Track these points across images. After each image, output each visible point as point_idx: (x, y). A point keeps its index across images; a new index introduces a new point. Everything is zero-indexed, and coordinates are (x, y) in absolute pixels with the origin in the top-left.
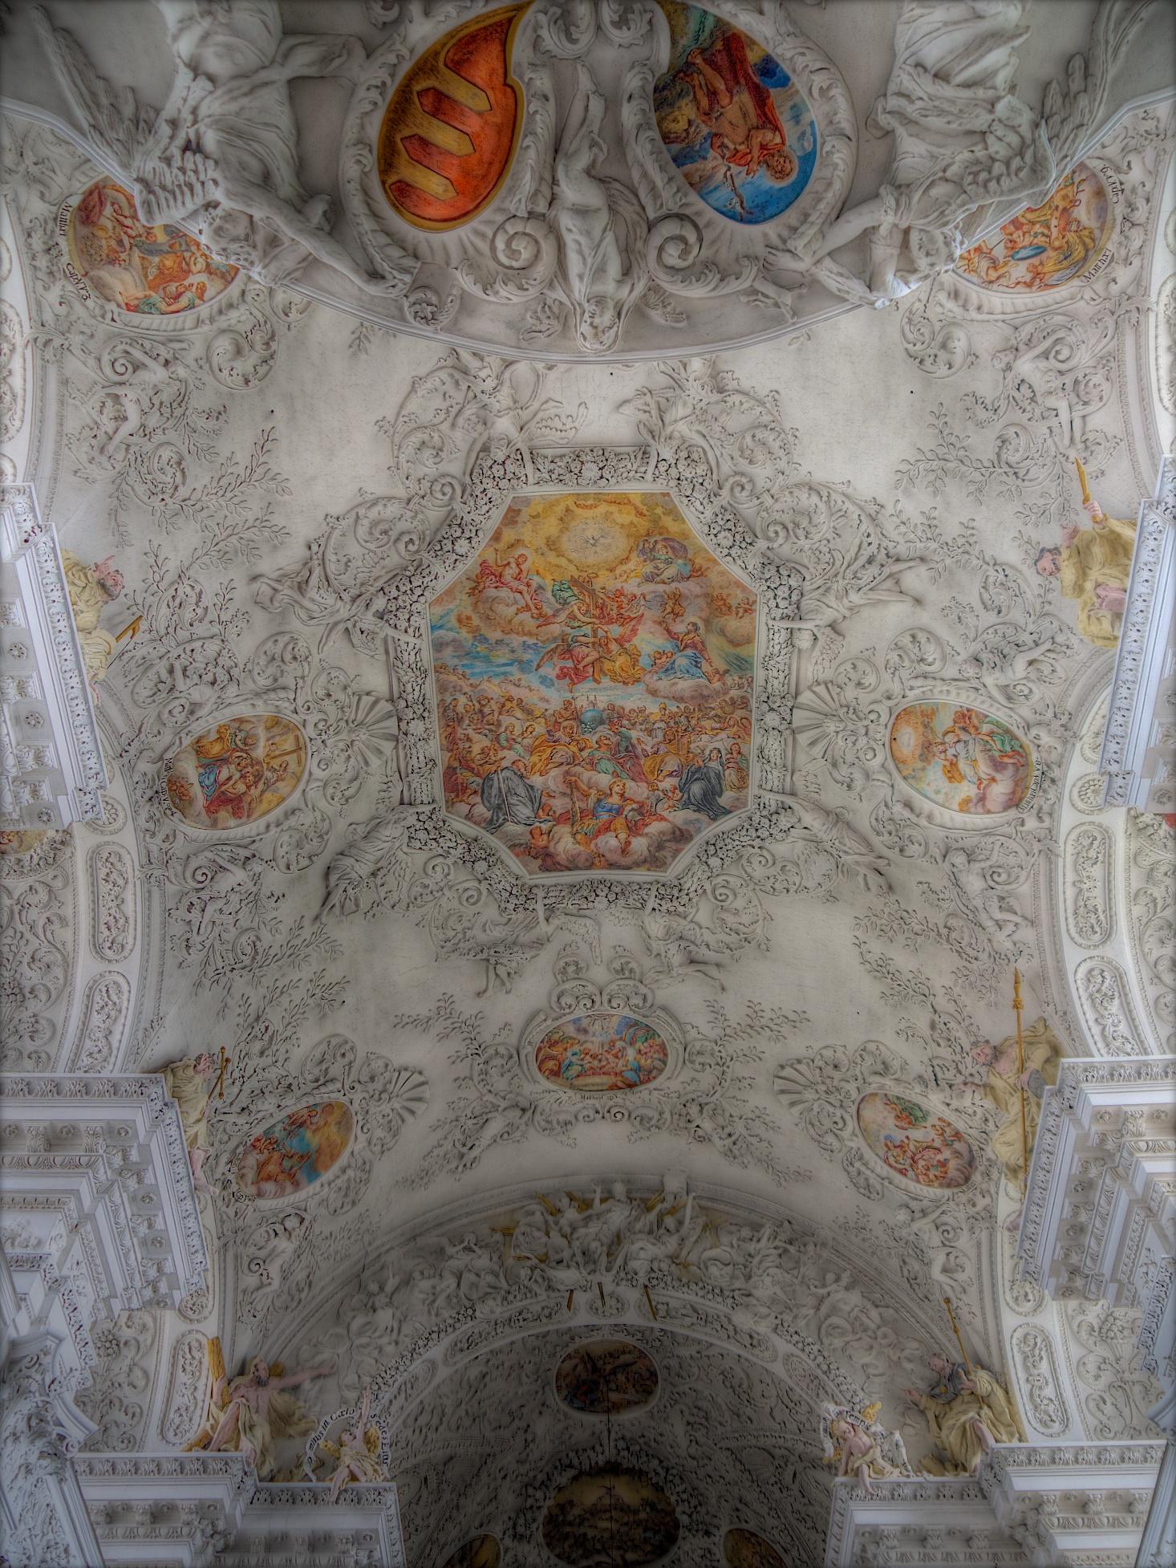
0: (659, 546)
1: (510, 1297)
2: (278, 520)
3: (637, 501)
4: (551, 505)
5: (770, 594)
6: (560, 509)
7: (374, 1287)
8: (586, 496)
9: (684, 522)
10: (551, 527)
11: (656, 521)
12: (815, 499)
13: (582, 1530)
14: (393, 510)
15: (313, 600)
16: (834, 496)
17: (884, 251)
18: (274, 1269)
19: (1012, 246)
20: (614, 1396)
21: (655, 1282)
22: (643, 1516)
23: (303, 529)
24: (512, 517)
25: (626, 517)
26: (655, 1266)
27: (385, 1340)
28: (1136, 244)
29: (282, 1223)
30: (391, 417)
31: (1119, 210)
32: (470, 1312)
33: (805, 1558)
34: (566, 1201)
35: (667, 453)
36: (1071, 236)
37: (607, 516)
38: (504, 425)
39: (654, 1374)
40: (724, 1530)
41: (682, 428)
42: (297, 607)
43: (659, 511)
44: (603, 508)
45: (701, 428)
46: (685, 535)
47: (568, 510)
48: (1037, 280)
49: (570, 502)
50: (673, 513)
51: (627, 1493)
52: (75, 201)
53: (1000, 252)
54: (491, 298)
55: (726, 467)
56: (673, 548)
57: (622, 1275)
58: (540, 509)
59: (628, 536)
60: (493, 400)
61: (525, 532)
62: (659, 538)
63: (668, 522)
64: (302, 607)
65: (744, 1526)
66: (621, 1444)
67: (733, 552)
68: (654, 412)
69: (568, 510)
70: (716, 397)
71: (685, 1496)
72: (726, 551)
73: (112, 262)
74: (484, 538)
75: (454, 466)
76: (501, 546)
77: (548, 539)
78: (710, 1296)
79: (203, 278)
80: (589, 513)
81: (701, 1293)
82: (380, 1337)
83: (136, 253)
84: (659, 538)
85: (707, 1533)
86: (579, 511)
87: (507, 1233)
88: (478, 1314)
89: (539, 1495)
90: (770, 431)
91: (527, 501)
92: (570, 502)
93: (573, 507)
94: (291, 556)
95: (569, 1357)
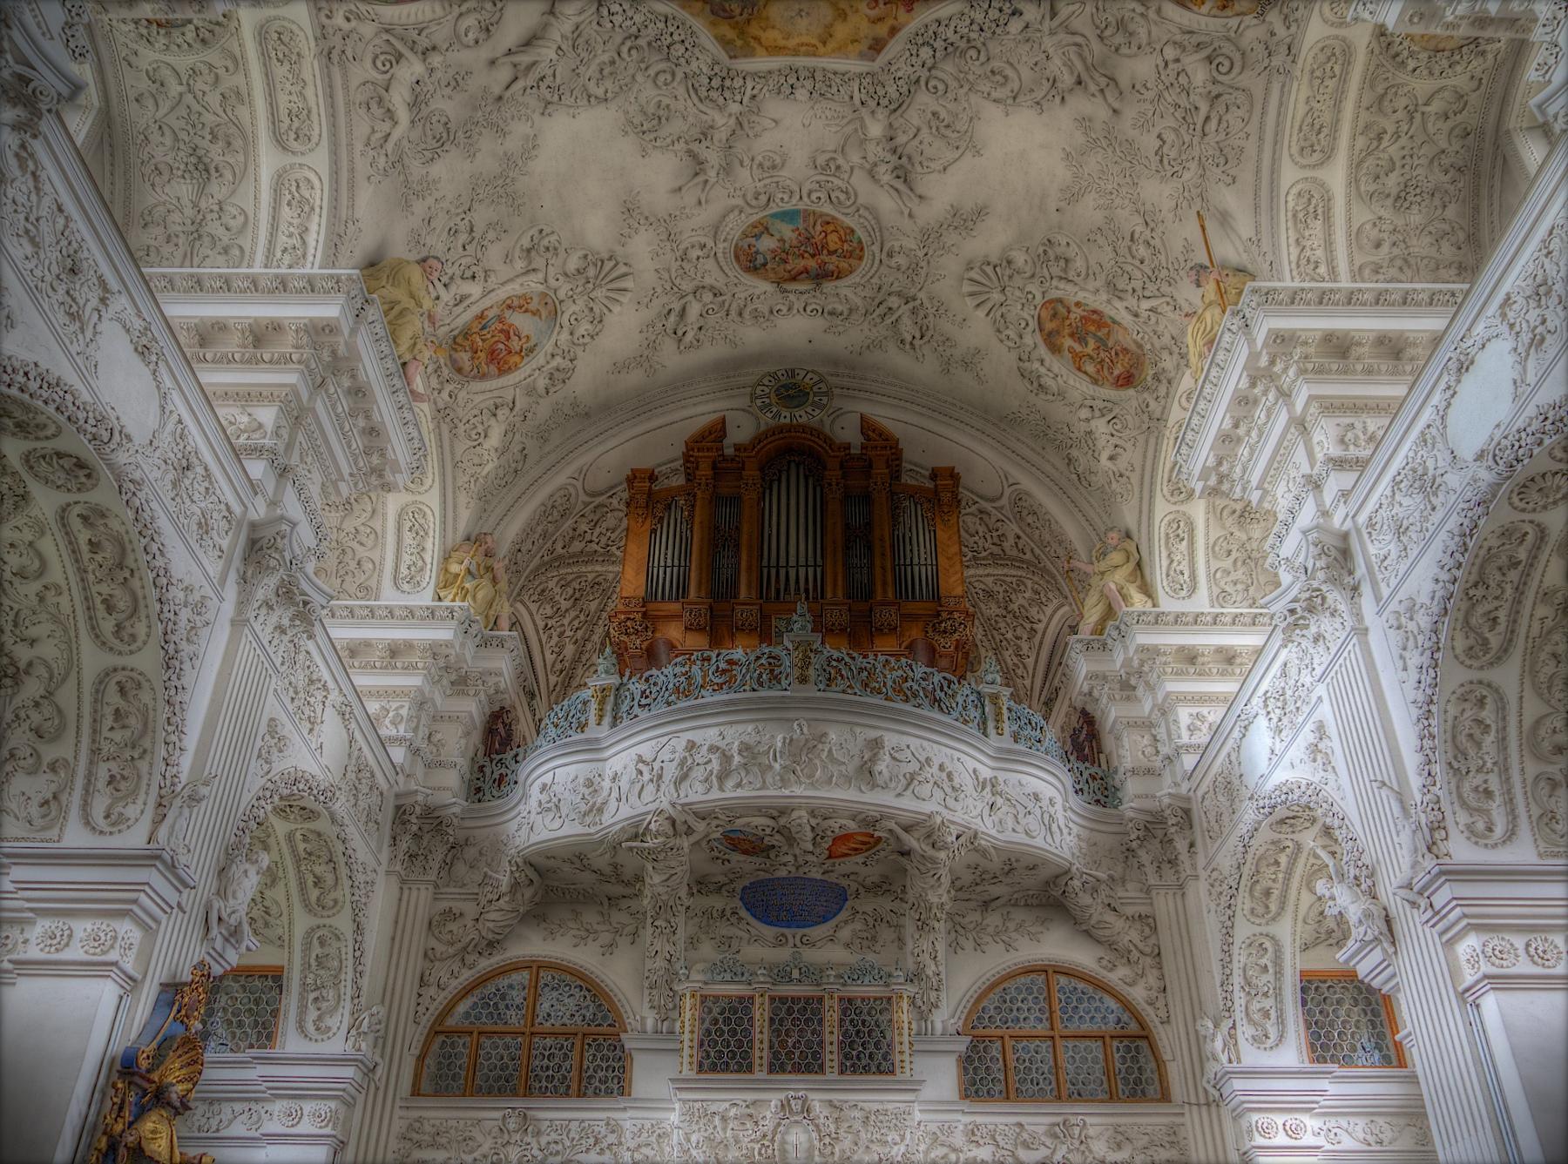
0: (738, 11)
2: (1080, 138)
3: (759, 50)
4: (841, 50)
5: (630, 14)
6: (832, 45)
8: (807, 54)
9: (716, 38)
10: (842, 31)
11: (742, 33)
12: (600, 92)
14: (985, 87)
15: (1071, 69)
16: (585, 102)
17: (681, 828)
19: (500, 319)
23: (1064, 117)
24: (877, 46)
25: (771, 36)
28: (430, 369)
30: (968, 155)
31: (445, 371)
35: (735, 108)
36: (467, 343)
37: (788, 36)
38: (876, 129)
41: (720, 120)
42: (1089, 61)
43: (739, 43)
44: (792, 43)
45: (705, 117)
46: (713, 24)
47: (824, 43)
48: (481, 316)
49: (822, 50)
50: (725, 42)
52: (1131, 392)
53: (508, 313)
54: (844, 822)
55: (681, 91)
56: (724, 10)
58: (850, 47)
59: (768, 18)
60: (882, 154)
61: (865, 29)
62: (738, 18)
63: (730, 34)
64: (1083, 60)
67: (669, 40)
68: (746, 125)
69: (824, 43)
70: (695, 147)
72: (676, 37)
73: (1126, 350)
74: (903, 35)
75: (923, 98)
76: (890, 22)
77: (845, 19)
79: (1073, 308)
80: (805, 39)
83: (1110, 344)
84: (738, 18)
86: (814, 41)
90: (648, 128)
91: (862, 56)
92: (822, 50)
93: (820, 45)
94: (1081, 104)
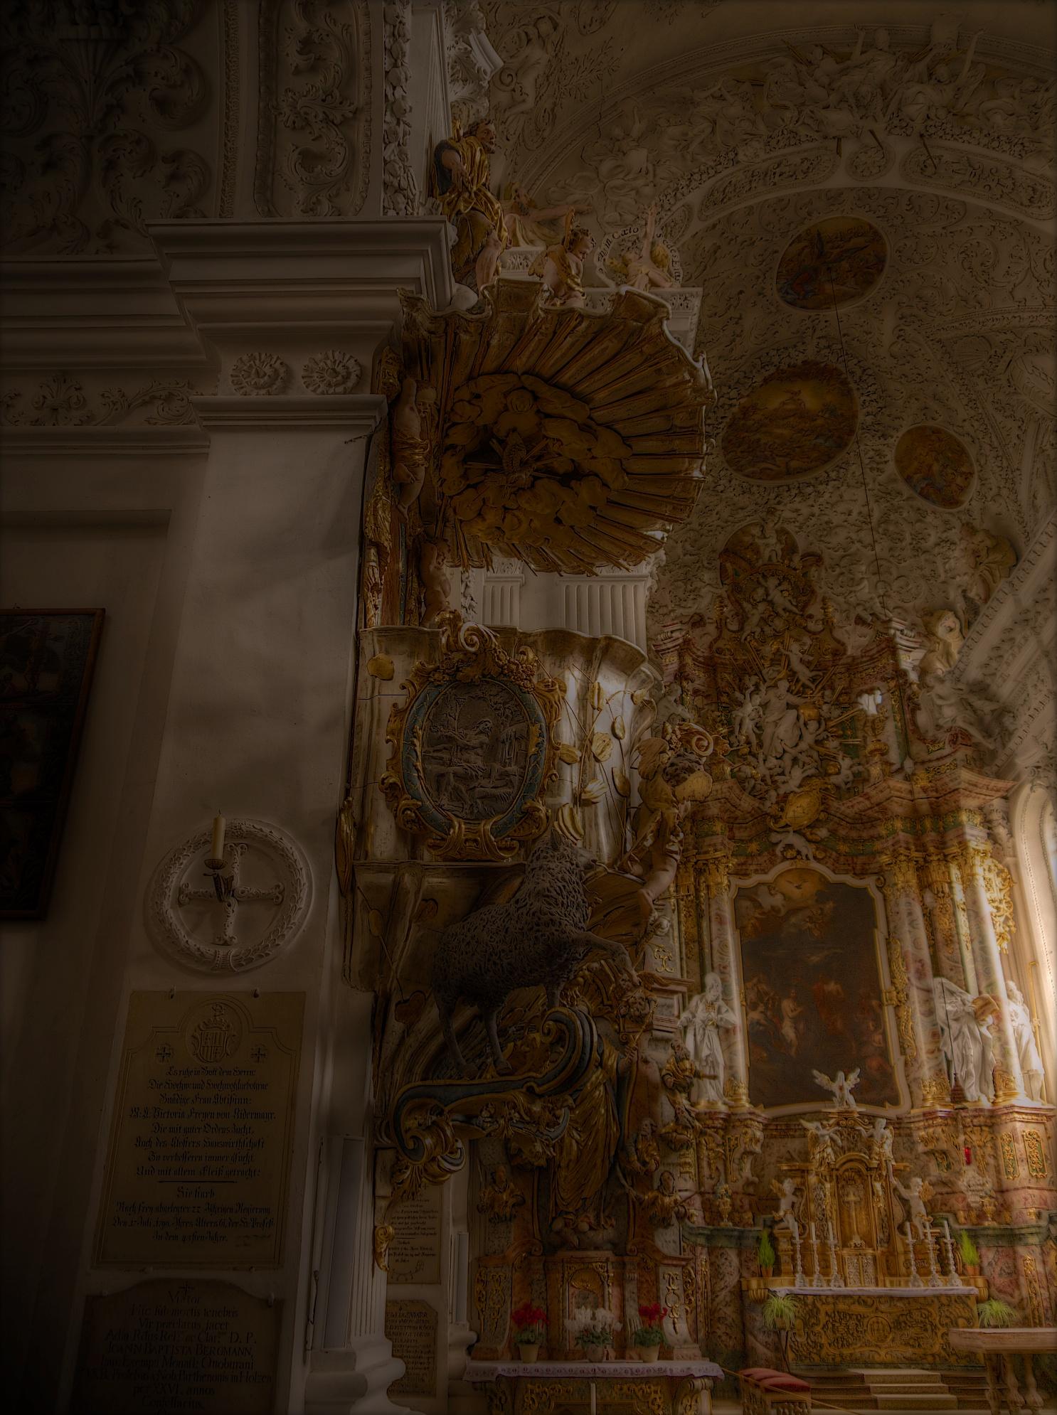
1: (773, 142)
7: (617, 132)
13: (758, 436)
18: (528, 83)
20: (828, 288)
21: (932, 130)
22: (819, 422)
26: (932, 115)
27: (640, 182)
29: (535, 25)
32: (731, 155)
33: (996, 444)
34: (819, 50)
39: (881, 261)
40: (904, 430)
51: (810, 398)
57: (896, 122)
65: (931, 423)
66: (823, 343)
71: (874, 397)
78: (995, 144)
81: (985, 141)
82: (635, 179)
85: (884, 436)
87: (757, 83)
88: (741, 157)
89: (733, 393)
95: (799, 239)
